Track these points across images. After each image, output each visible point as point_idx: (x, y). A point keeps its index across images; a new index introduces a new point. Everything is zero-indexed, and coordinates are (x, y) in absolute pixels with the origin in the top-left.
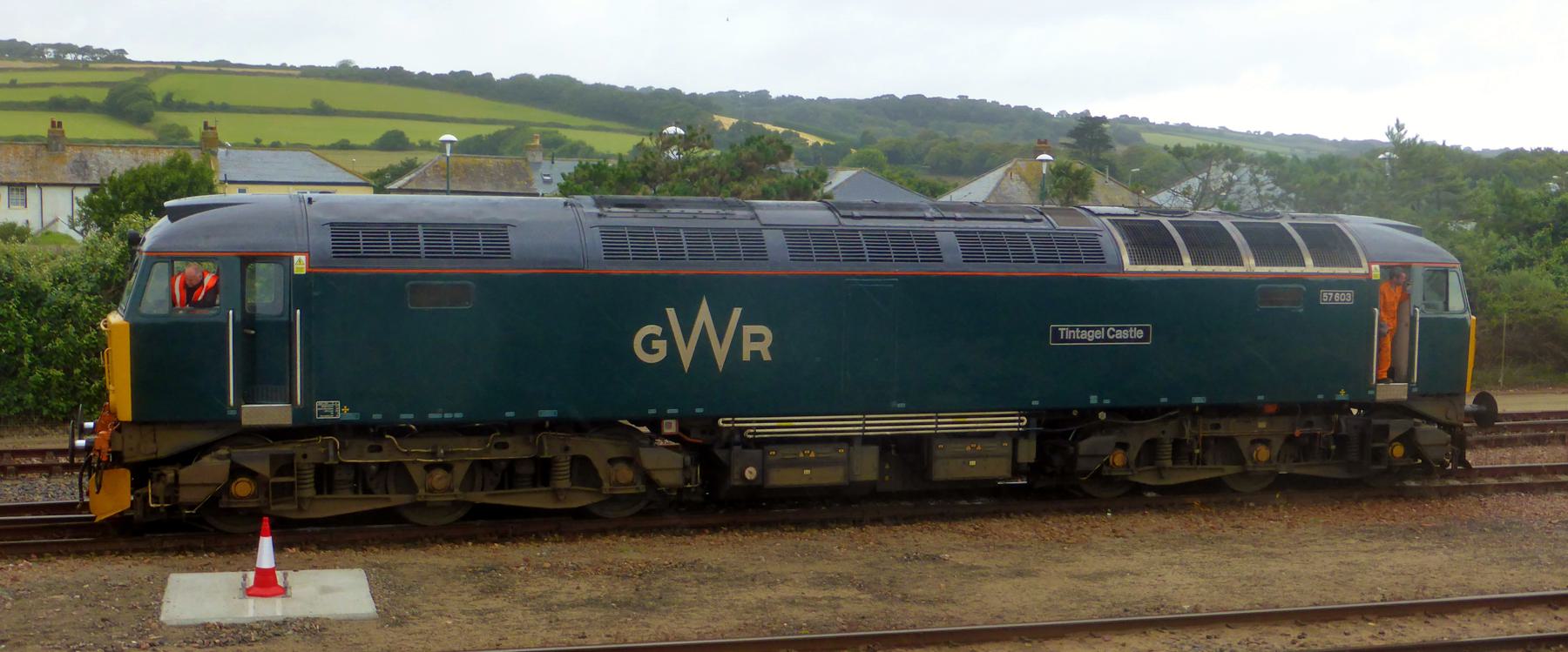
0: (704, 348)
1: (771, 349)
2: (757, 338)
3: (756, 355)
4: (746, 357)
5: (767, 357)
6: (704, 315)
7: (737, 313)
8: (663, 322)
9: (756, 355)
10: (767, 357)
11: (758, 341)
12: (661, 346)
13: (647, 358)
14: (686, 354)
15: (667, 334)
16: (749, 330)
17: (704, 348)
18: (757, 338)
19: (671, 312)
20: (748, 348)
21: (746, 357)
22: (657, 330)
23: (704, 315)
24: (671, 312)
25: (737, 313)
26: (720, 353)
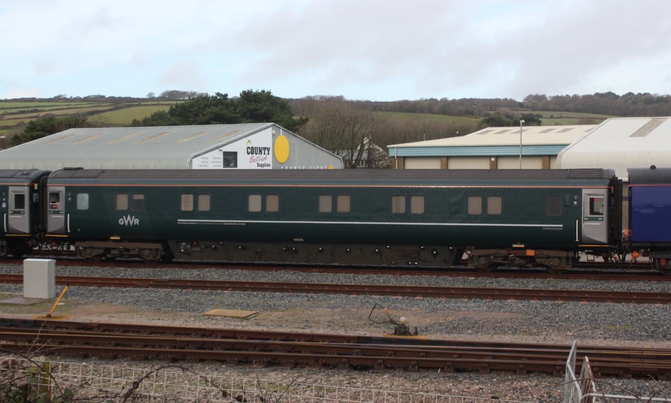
0: (129, 222)
1: (139, 223)
2: (136, 221)
3: (136, 224)
4: (135, 224)
5: (138, 224)
6: (129, 218)
7: (133, 217)
8: (123, 218)
9: (136, 224)
10: (138, 224)
11: (137, 221)
12: (123, 222)
13: (120, 222)
14: (126, 223)
15: (124, 220)
16: (135, 220)
17: (129, 222)
18: (136, 221)
19: (124, 217)
20: (135, 223)
21: (135, 224)
22: (122, 219)
23: (129, 218)
24: (124, 217)
25: (133, 217)
26: (131, 223)
